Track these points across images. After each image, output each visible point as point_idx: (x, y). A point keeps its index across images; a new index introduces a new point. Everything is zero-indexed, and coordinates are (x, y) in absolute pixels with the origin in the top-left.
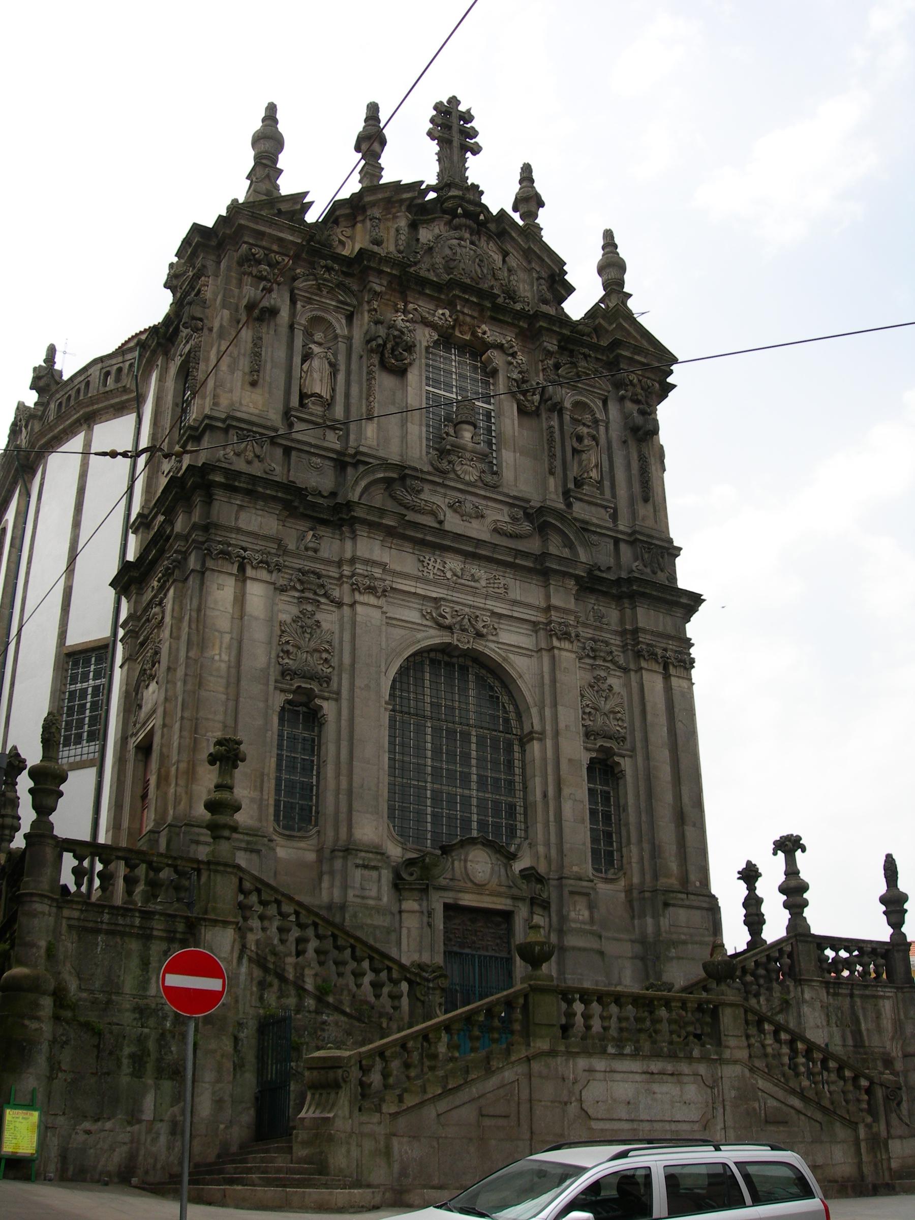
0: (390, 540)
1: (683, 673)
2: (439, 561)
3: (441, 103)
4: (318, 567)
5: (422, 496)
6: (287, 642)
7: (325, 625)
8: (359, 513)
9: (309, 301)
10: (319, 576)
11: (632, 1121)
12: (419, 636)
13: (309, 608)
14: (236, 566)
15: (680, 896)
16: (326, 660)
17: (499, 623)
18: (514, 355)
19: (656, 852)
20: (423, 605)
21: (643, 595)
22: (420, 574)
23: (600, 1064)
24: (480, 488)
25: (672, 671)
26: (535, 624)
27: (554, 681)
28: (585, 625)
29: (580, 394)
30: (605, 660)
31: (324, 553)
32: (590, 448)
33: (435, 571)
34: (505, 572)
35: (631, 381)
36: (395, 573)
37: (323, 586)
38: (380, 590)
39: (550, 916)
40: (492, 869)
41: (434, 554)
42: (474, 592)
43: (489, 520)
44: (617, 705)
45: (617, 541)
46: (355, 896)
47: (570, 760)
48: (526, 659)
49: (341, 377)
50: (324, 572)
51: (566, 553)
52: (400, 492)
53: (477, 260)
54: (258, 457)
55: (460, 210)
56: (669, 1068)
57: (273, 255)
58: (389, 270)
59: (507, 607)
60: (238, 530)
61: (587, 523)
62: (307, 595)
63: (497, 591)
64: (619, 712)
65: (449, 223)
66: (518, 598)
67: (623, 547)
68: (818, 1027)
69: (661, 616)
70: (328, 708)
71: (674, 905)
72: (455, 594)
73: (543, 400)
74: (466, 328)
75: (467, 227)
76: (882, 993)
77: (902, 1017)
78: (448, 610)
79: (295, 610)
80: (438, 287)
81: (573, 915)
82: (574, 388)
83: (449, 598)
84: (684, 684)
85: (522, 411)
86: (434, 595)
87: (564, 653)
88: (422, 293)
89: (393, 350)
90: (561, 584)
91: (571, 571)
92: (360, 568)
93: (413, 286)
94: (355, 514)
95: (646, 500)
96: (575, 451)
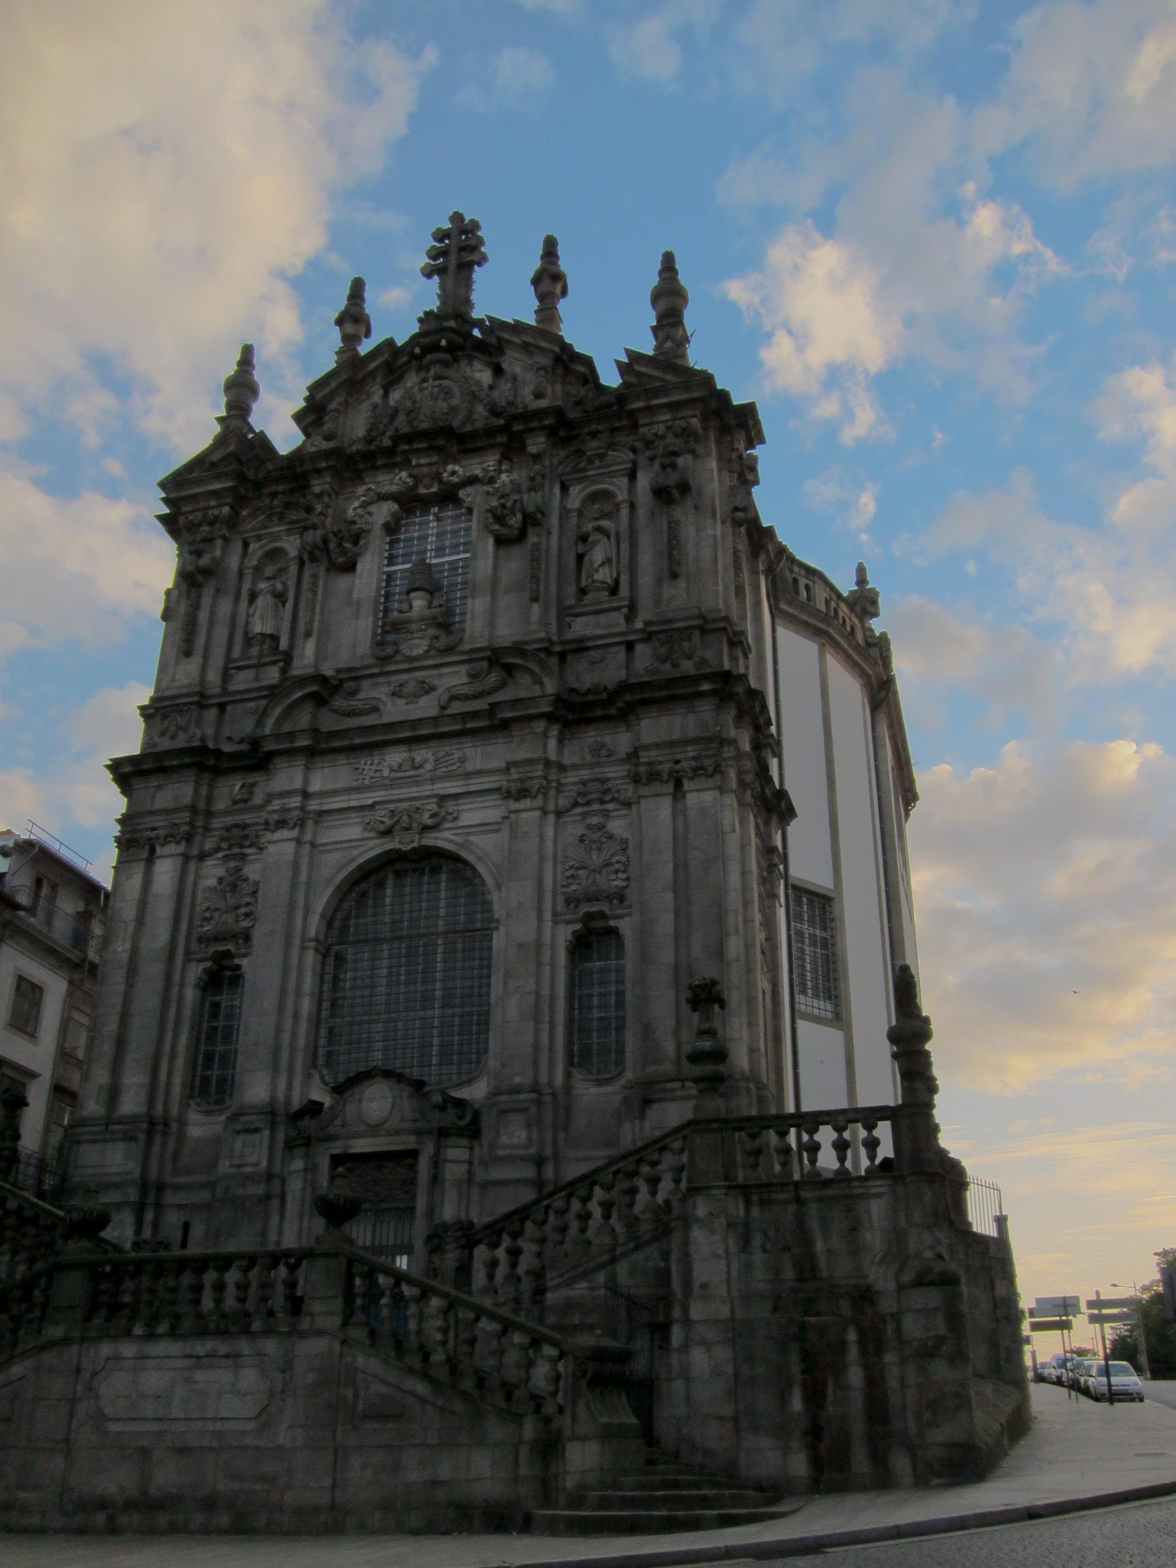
0: (318, 759)
1: (702, 782)
2: (376, 761)
3: (439, 230)
4: (248, 818)
5: (362, 695)
6: (208, 909)
7: (253, 877)
8: (269, 746)
9: (259, 538)
10: (245, 826)
11: (161, 1419)
12: (355, 853)
13: (232, 864)
14: (147, 848)
15: (670, 1085)
16: (247, 915)
17: (457, 805)
18: (491, 481)
19: (647, 1031)
20: (363, 816)
21: (645, 702)
22: (355, 784)
23: (128, 1349)
24: (433, 657)
25: (687, 785)
26: (498, 790)
27: (510, 852)
28: (576, 767)
29: (594, 482)
30: (602, 802)
31: (258, 799)
32: (595, 543)
33: (372, 775)
34: (461, 743)
35: (656, 435)
36: (322, 794)
37: (246, 837)
38: (291, 823)
39: (481, 1146)
40: (393, 1105)
41: (372, 755)
42: (416, 781)
43: (440, 690)
44: (612, 855)
45: (630, 646)
46: (232, 1166)
47: (521, 946)
48: (492, 835)
49: (289, 605)
50: (254, 821)
51: (537, 690)
52: (339, 702)
53: (442, 396)
54: (181, 728)
55: (417, 350)
56: (223, 1348)
57: (210, 512)
58: (324, 465)
59: (461, 783)
60: (152, 813)
61: (580, 640)
62: (236, 850)
63: (450, 768)
64: (618, 862)
65: (419, 369)
66: (478, 767)
67: (640, 649)
68: (718, 1256)
69: (678, 720)
70: (244, 962)
71: (660, 1100)
72: (394, 792)
73: (526, 516)
74: (427, 481)
75: (433, 363)
76: (860, 1191)
77: (903, 1222)
78: (383, 813)
79: (221, 872)
80: (391, 452)
81: (504, 1139)
82: (580, 480)
83: (388, 798)
84: (708, 796)
85: (500, 542)
86: (370, 802)
87: (524, 815)
88: (376, 468)
89: (340, 545)
90: (527, 731)
91: (532, 711)
92: (276, 805)
93: (361, 466)
94: (266, 749)
95: (674, 576)
96: (580, 558)
